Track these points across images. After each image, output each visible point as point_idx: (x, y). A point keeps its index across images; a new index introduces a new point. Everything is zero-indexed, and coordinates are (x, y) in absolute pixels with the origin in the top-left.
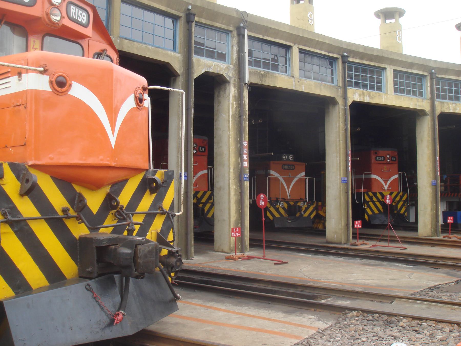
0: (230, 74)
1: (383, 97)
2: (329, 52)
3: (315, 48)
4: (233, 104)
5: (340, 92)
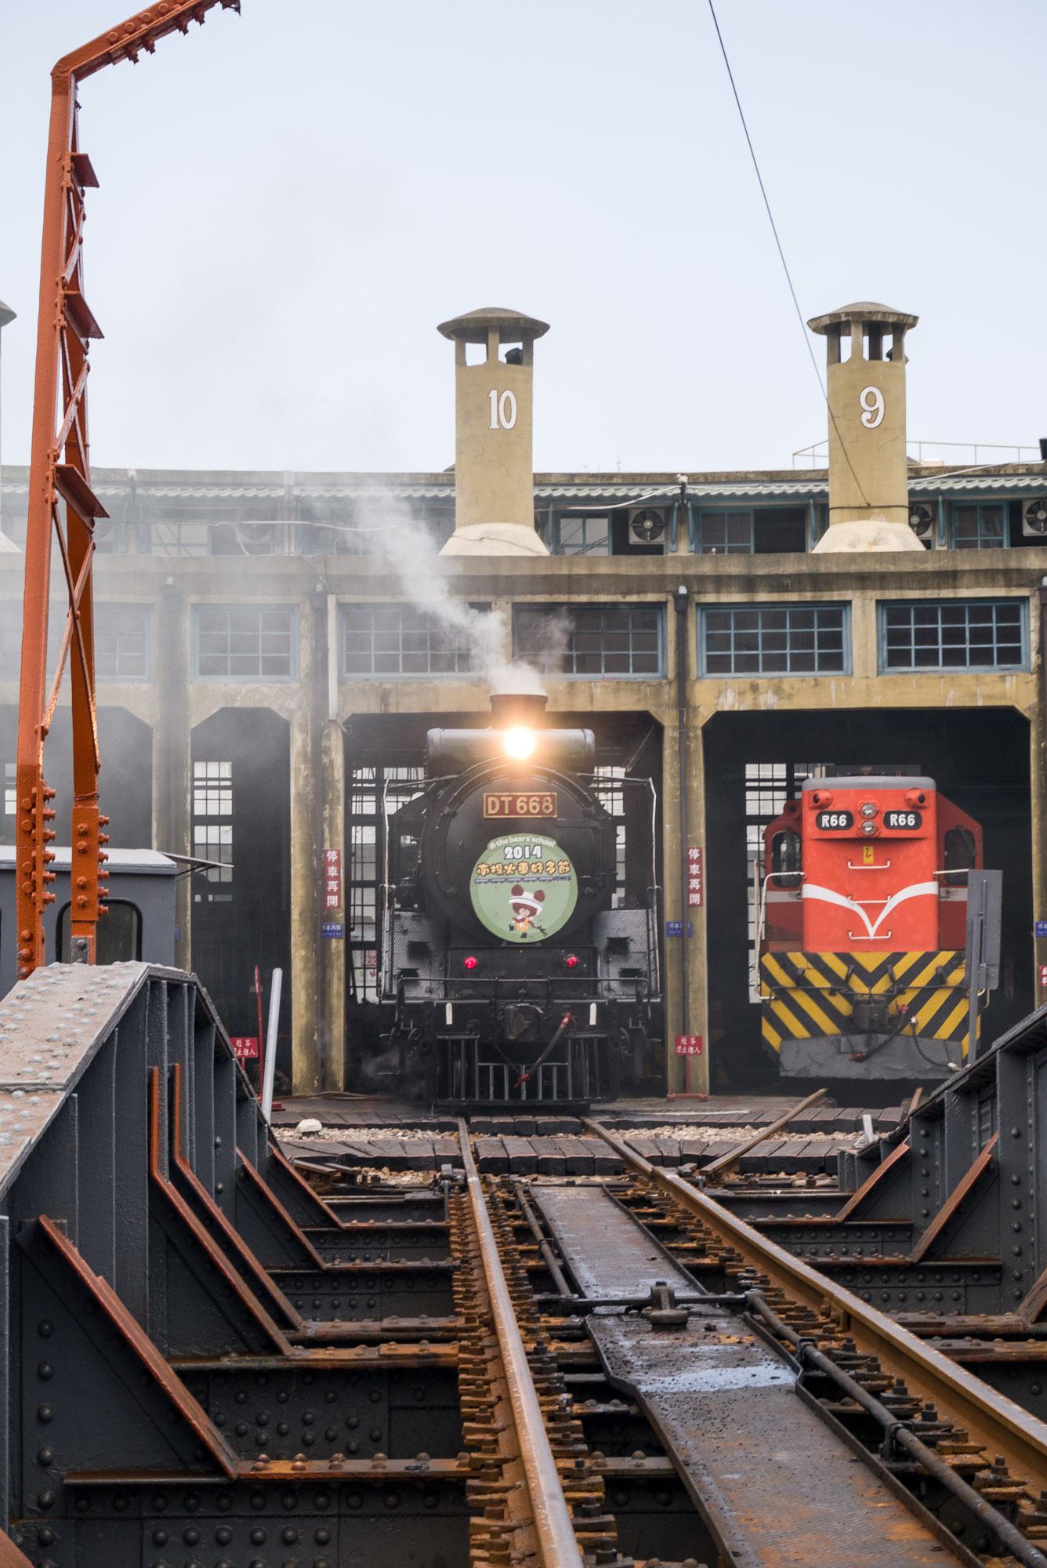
0: (293, 705)
1: (833, 687)
2: (625, 594)
3: (570, 592)
4: (298, 770)
5: (669, 693)
